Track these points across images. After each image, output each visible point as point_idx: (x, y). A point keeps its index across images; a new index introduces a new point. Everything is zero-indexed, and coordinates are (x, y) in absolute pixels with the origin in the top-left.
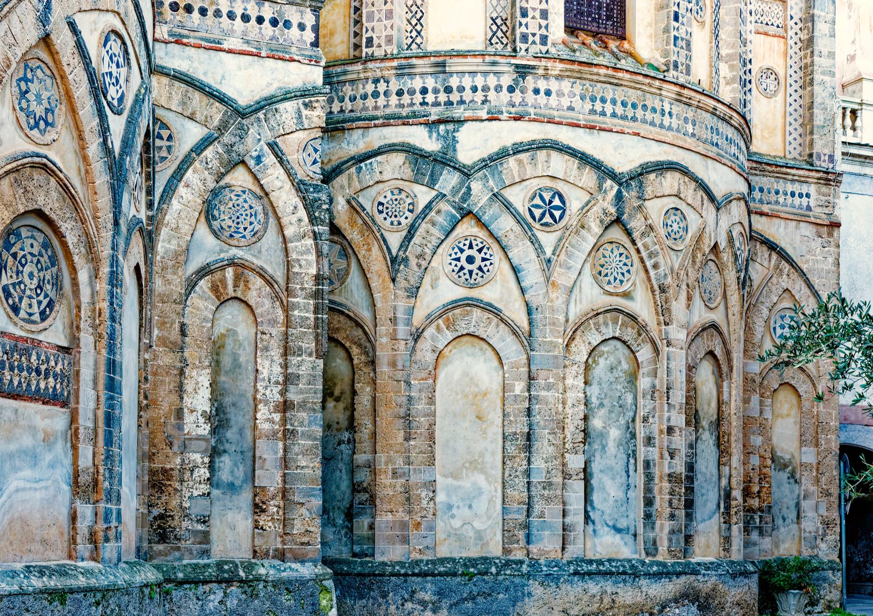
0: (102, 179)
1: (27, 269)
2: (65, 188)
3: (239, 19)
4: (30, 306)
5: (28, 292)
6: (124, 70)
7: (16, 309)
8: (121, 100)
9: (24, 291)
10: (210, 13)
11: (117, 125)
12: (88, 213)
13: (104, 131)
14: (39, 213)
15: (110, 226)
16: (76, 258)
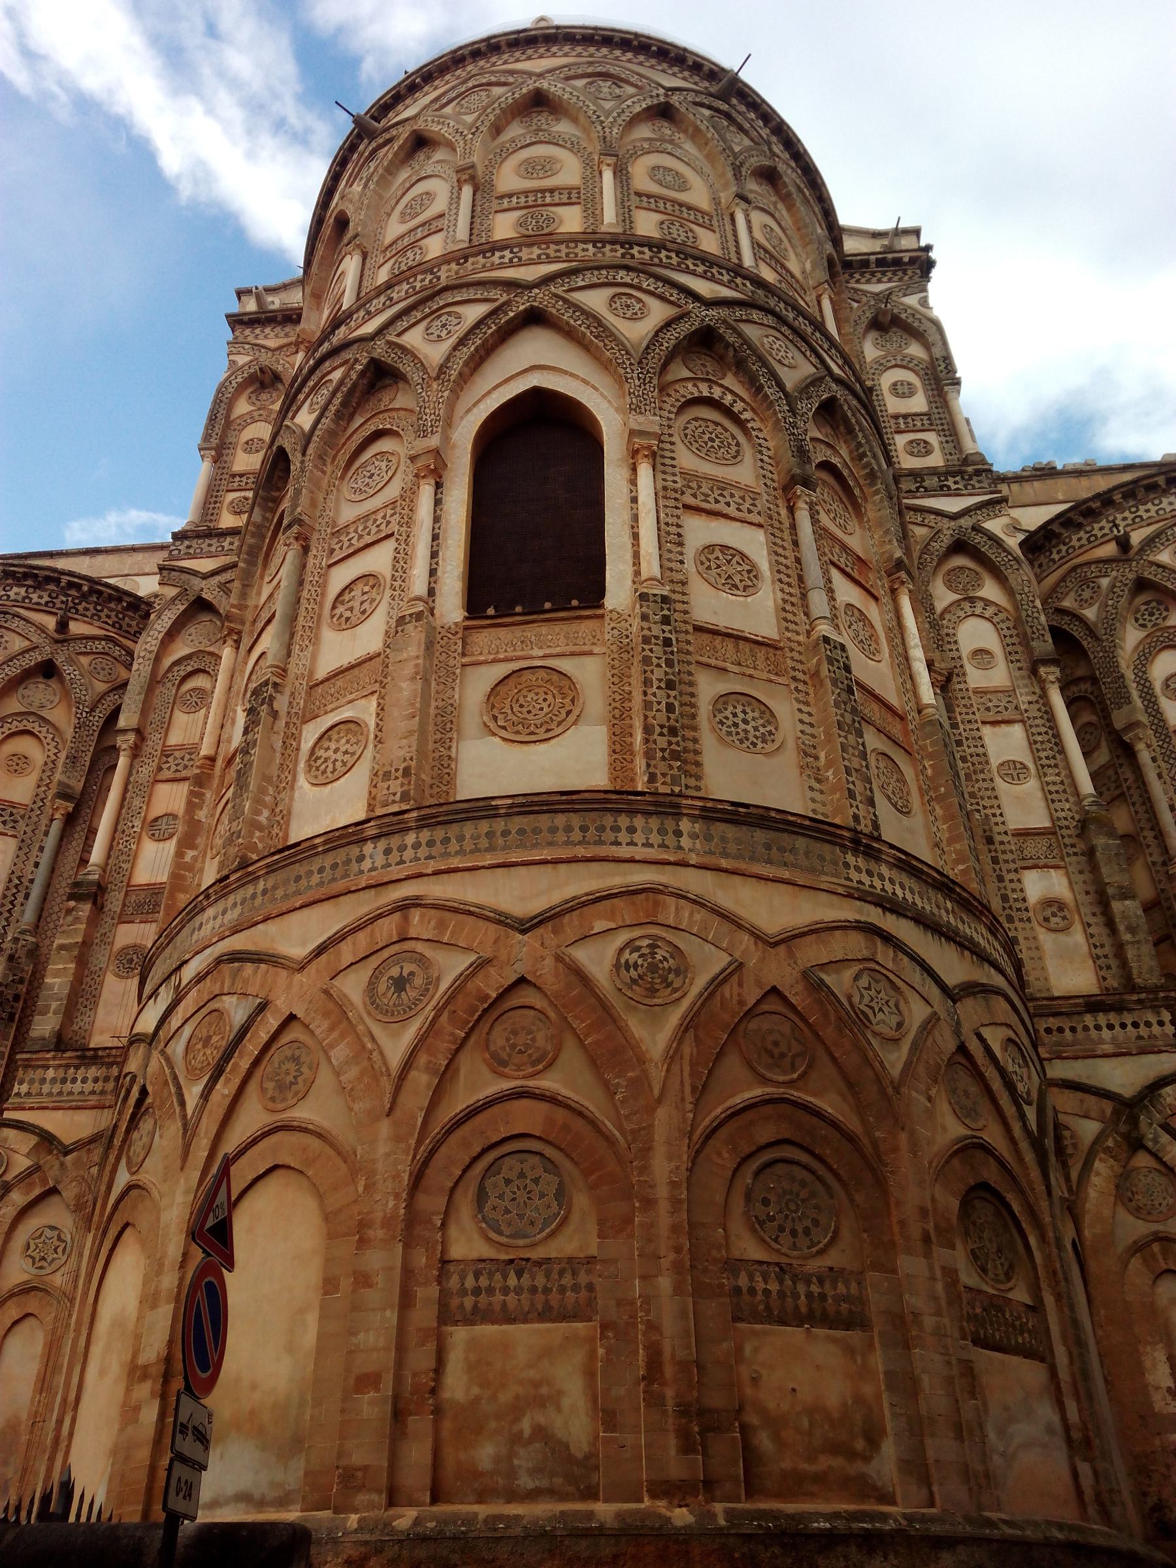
0: (1029, 1157)
1: (986, 1235)
2: (1001, 1162)
3: (1105, 1029)
4: (996, 1267)
5: (992, 1256)
6: (1025, 1070)
7: (984, 1270)
8: (1028, 1093)
9: (987, 1254)
10: (1079, 1029)
11: (1031, 1113)
12: (1024, 1184)
13: (1022, 1116)
14: (984, 1186)
15: (1045, 1196)
16: (1024, 1225)
